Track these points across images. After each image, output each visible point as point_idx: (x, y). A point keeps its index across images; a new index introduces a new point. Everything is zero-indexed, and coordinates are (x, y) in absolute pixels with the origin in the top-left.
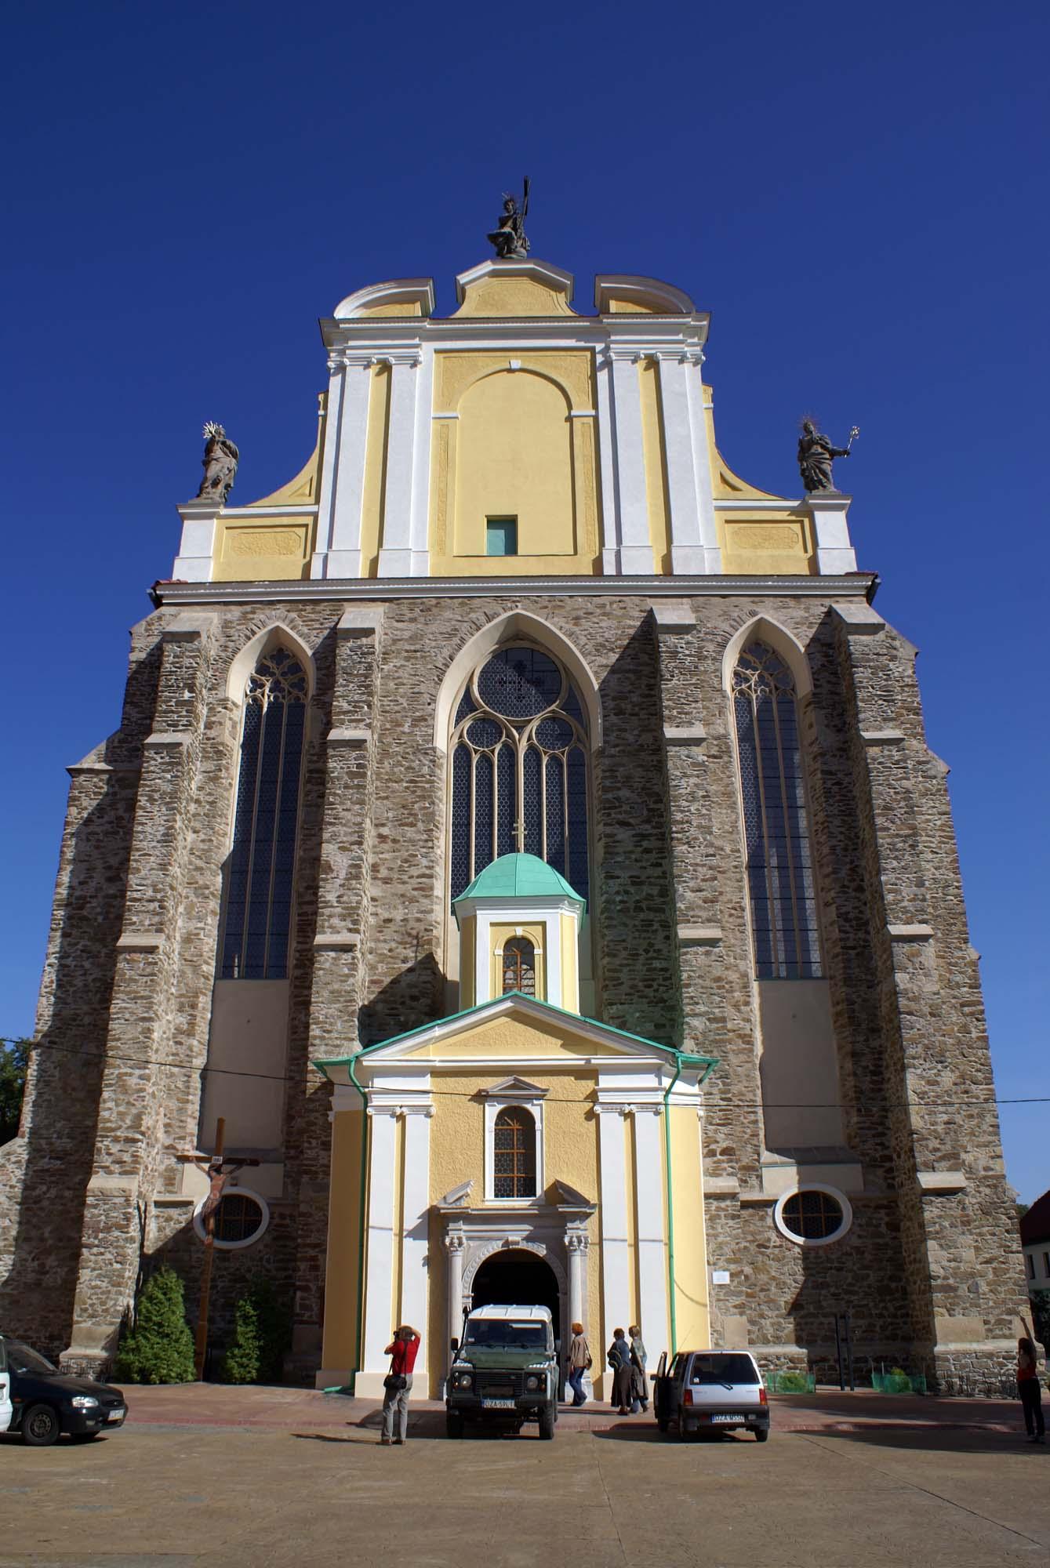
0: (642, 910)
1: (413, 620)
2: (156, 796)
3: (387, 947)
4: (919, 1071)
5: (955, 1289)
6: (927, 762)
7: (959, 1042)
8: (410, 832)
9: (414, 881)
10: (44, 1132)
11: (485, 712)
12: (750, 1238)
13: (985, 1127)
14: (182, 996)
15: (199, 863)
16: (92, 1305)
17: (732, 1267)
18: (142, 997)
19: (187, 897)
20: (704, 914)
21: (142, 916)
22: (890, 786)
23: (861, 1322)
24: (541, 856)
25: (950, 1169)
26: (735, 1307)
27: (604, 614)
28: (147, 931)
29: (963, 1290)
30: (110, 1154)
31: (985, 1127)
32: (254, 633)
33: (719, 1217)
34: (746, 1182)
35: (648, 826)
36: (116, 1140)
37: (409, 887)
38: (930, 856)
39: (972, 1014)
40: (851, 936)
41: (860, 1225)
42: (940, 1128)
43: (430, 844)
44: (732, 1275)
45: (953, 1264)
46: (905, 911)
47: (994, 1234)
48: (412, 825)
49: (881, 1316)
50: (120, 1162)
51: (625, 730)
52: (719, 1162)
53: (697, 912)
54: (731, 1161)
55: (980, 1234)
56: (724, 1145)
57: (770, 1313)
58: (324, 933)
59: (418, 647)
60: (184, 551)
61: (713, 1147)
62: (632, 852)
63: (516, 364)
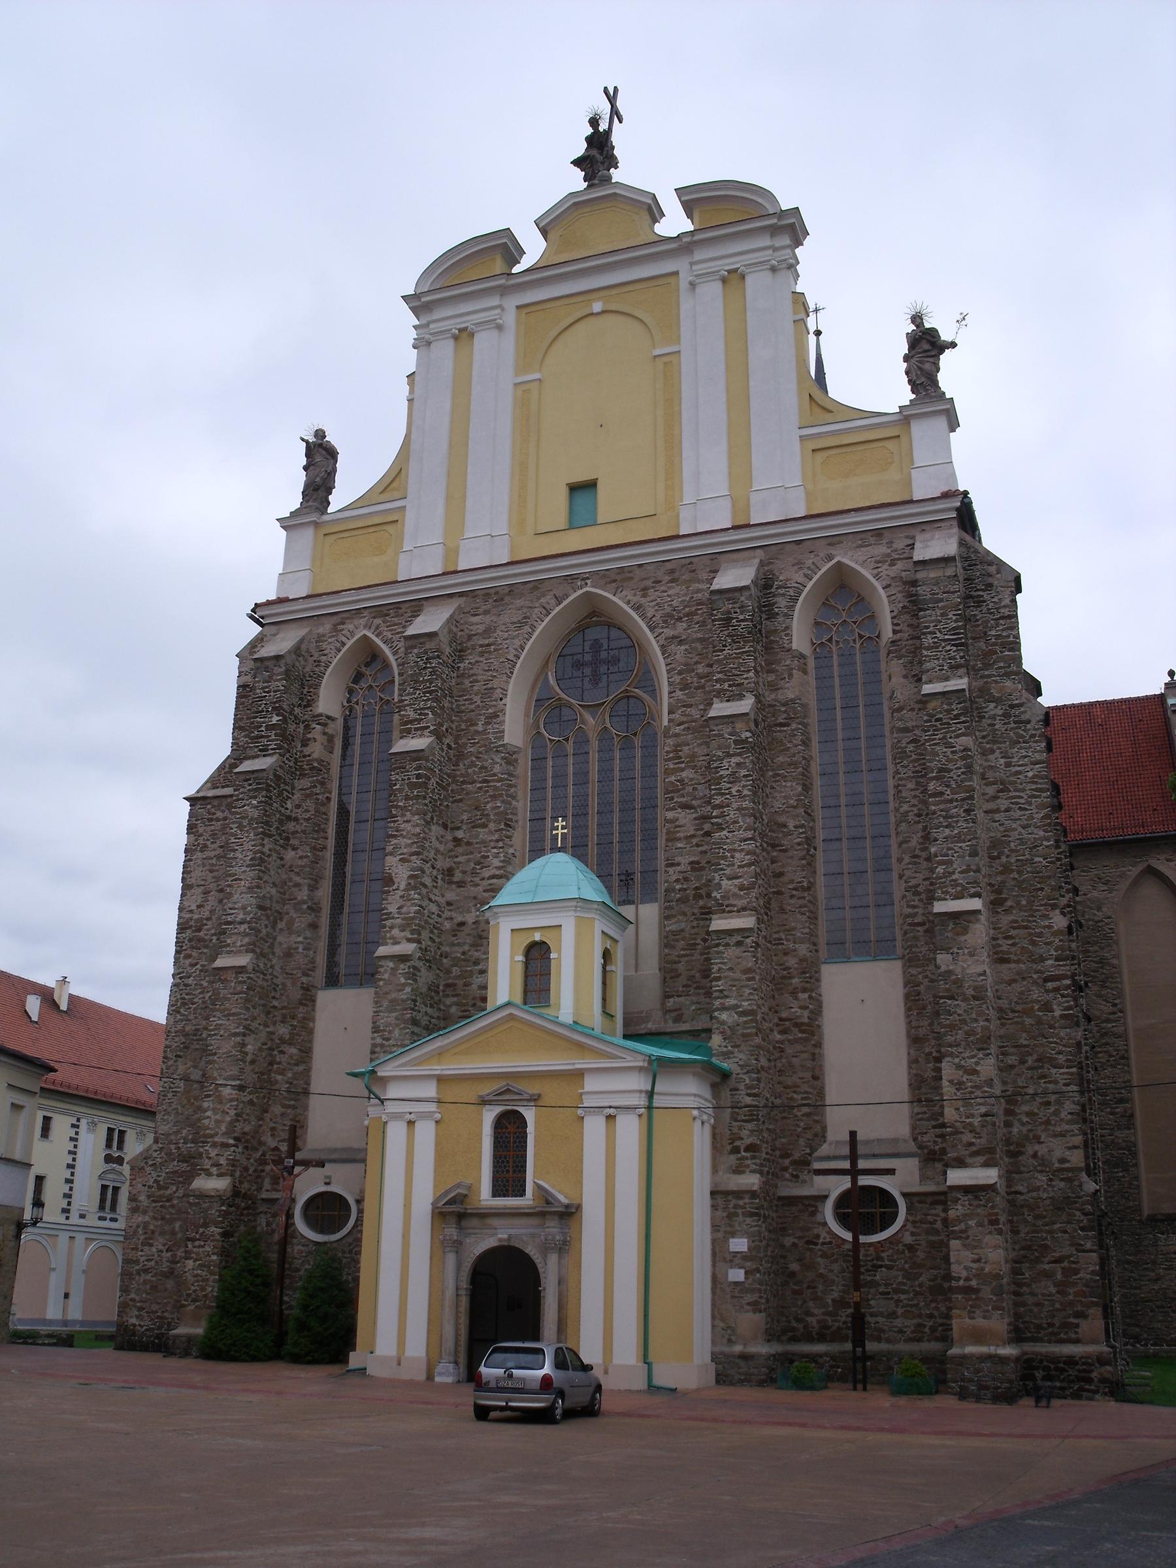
0: (701, 897)
1: (486, 612)
2: (245, 823)
3: (461, 950)
4: (957, 1060)
5: (977, 1291)
6: (1020, 705)
7: (1039, 1022)
9: (485, 883)
12: (799, 1234)
13: (1063, 1115)
16: (195, 1291)
17: (749, 1264)
18: (234, 1014)
20: (740, 903)
21: (234, 938)
23: (908, 1322)
26: (748, 1304)
27: (672, 581)
28: (240, 952)
29: (986, 1292)
30: (209, 1158)
32: (344, 644)
33: (736, 1214)
34: (797, 1177)
35: (709, 808)
36: (214, 1145)
37: (481, 889)
38: (1019, 813)
39: (1056, 990)
40: (920, 911)
41: (914, 1222)
42: (976, 1121)
44: (746, 1273)
46: (955, 883)
47: (1066, 1232)
48: (484, 826)
49: (931, 1316)
50: (217, 1165)
51: (691, 706)
52: (743, 1158)
53: (731, 901)
54: (753, 1158)
55: (1050, 1232)
56: (748, 1141)
57: (816, 1311)
58: (386, 944)
59: (491, 640)
61: (737, 1143)
62: (693, 836)
63: (597, 307)
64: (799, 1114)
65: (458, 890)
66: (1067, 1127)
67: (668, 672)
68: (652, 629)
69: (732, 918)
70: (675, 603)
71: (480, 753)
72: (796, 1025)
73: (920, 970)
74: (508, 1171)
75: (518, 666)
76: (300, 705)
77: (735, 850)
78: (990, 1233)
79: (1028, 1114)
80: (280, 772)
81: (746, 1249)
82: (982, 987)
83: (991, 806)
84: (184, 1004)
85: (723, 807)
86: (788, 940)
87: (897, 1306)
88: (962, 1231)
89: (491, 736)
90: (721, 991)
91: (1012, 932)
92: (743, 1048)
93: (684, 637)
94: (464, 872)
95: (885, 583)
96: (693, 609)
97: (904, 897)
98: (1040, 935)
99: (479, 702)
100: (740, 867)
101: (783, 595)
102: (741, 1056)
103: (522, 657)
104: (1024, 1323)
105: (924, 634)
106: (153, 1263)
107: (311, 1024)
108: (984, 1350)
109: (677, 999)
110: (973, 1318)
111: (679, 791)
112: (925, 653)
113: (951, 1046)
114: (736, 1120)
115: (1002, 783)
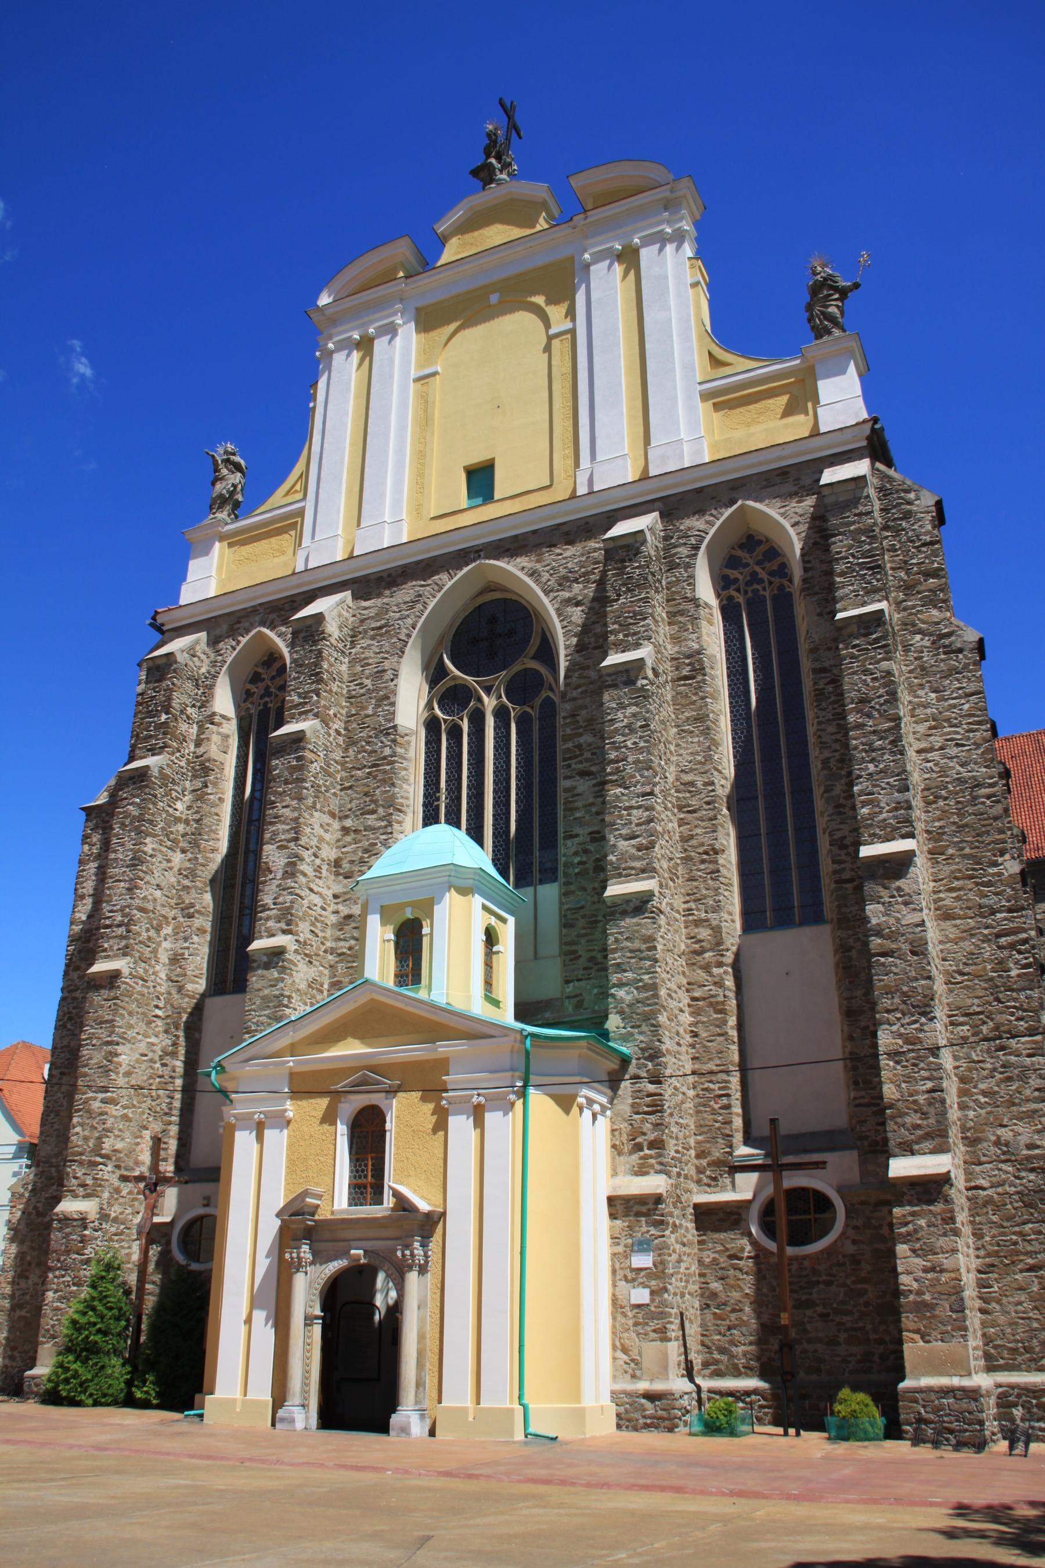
3: (347, 945)
4: (894, 1028)
8: (371, 820)
10: (54, 1160)
11: (455, 678)
12: (720, 1248)
14: (168, 1017)
15: (186, 882)
16: (53, 1326)
17: (653, 1283)
18: (107, 1022)
19: (174, 919)
22: (866, 672)
24: (459, 827)
25: (934, 1151)
28: (116, 956)
30: (76, 1178)
31: (1028, 1092)
36: (81, 1163)
40: (847, 866)
41: (856, 1228)
43: (389, 830)
44: (652, 1293)
45: (929, 1276)
46: (884, 825)
48: (373, 812)
49: (880, 1342)
50: (84, 1185)
52: (645, 1157)
58: (261, 937)
60: (189, 578)
61: (639, 1140)
62: (592, 804)
64: (716, 1106)
65: (346, 881)
66: (1034, 1106)
67: (565, 634)
68: (547, 593)
69: (628, 882)
70: (570, 565)
71: (371, 737)
72: (711, 1004)
73: (851, 932)
74: (366, 1177)
75: (409, 645)
76: (194, 706)
77: (631, 807)
78: (945, 1235)
79: (984, 1093)
80: (168, 771)
81: (651, 1265)
82: (921, 939)
83: (923, 745)
84: (70, 1019)
85: (617, 762)
86: (698, 910)
87: (839, 1331)
88: (909, 1234)
89: (381, 719)
90: (618, 965)
91: (956, 884)
92: (644, 1028)
93: (580, 598)
94: (352, 862)
95: (793, 520)
96: (589, 569)
97: (831, 850)
98: (989, 884)
99: (370, 686)
100: (637, 825)
101: (685, 544)
102: (641, 1038)
103: (414, 635)
104: (995, 1347)
105: (837, 559)
106: (28, 1297)
107: (197, 1035)
108: (944, 1381)
109: (577, 984)
110: (928, 1342)
111: (576, 757)
112: (838, 579)
113: (888, 1011)
114: (637, 1113)
115: (934, 720)
